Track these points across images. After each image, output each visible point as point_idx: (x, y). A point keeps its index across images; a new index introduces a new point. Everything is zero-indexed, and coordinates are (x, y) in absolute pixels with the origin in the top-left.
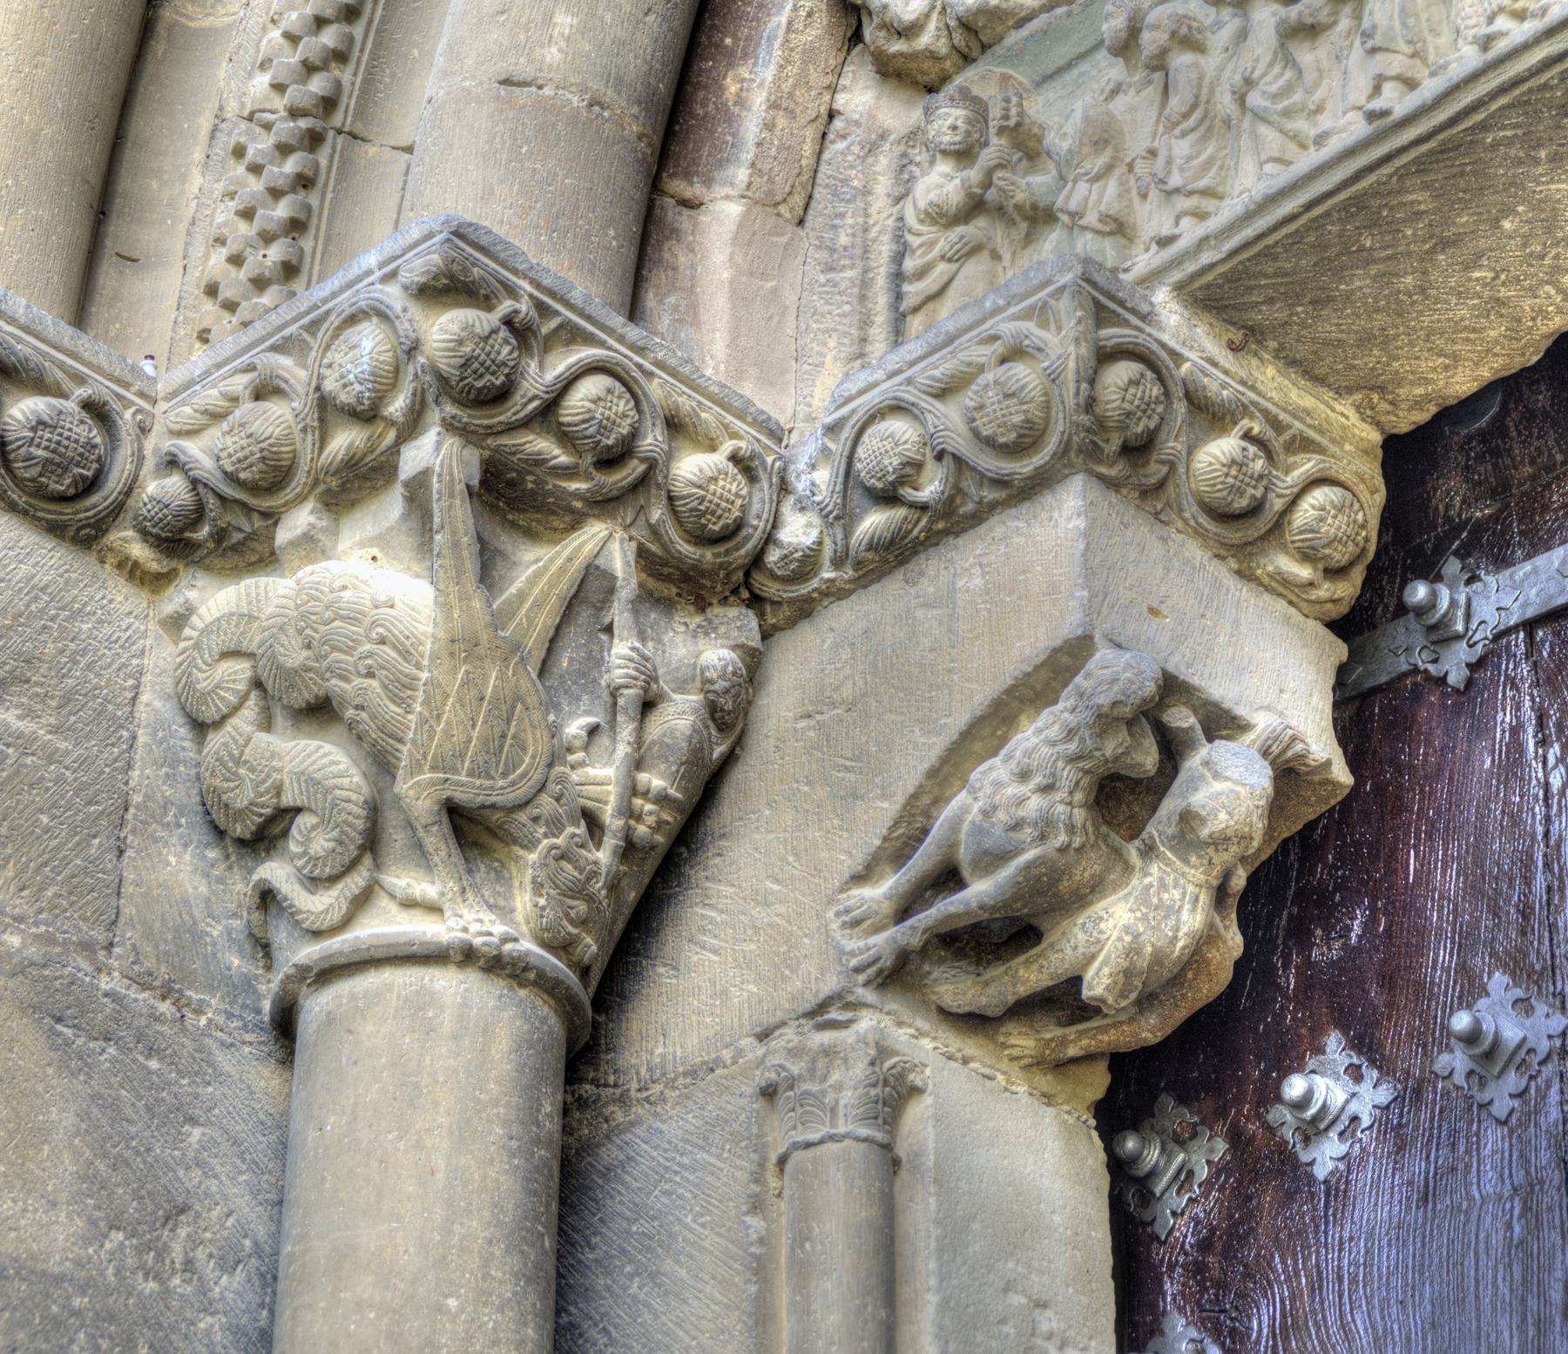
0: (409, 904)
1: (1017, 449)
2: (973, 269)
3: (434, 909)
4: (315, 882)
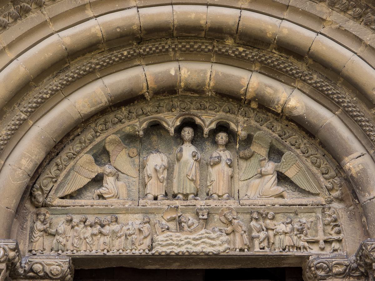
1: (54, 276)
2: (41, 238)
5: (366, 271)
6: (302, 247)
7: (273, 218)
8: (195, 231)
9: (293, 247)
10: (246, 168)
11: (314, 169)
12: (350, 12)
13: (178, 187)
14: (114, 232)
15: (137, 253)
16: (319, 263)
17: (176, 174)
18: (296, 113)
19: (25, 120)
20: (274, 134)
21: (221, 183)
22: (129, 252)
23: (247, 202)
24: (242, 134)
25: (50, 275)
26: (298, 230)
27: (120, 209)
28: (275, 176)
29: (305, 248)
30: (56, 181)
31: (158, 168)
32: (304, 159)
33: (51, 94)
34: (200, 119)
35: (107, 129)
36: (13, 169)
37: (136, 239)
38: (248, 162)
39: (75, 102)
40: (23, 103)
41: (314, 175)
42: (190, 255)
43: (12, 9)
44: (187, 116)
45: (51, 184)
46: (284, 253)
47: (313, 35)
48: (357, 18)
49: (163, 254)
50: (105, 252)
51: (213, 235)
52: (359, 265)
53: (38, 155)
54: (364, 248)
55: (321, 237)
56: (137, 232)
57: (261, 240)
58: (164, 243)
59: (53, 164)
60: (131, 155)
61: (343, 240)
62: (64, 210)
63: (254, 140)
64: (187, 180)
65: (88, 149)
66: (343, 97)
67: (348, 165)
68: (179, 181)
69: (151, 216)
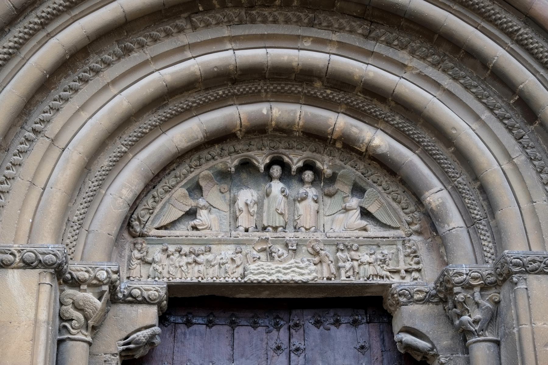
0: (83, 334)
1: (152, 300)
2: (139, 266)
3: (86, 336)
4: (73, 328)
5: (445, 296)
6: (385, 276)
7: (357, 250)
8: (285, 260)
9: (377, 276)
10: (331, 205)
11: (395, 205)
12: (429, 59)
13: (268, 220)
14: (208, 261)
15: (230, 280)
16: (401, 290)
17: (265, 208)
18: (379, 151)
19: (125, 152)
20: (357, 172)
21: (308, 217)
22: (223, 280)
23: (334, 235)
24: (328, 172)
25: (148, 300)
26: (381, 261)
27: (213, 240)
28: (359, 211)
29: (387, 277)
30: (152, 213)
31: (249, 202)
32: (385, 195)
33: (151, 130)
34: (289, 157)
35: (200, 165)
36: (114, 198)
37: (229, 268)
38: (333, 199)
39: (173, 137)
40: (124, 136)
41: (394, 210)
42: (281, 283)
43: (117, 49)
44: (276, 155)
45: (147, 216)
46: (368, 282)
47: (397, 78)
48: (435, 65)
49: (255, 282)
50: (200, 279)
51: (302, 265)
52: (439, 291)
53: (138, 186)
54: (446, 273)
55: (402, 267)
56: (230, 262)
57: (347, 269)
58: (256, 272)
59: (150, 196)
60: (222, 190)
61: (422, 270)
62: (160, 240)
63: (338, 178)
64: (277, 213)
65: (183, 183)
66: (423, 137)
67: (428, 199)
68: (268, 215)
69: (243, 247)
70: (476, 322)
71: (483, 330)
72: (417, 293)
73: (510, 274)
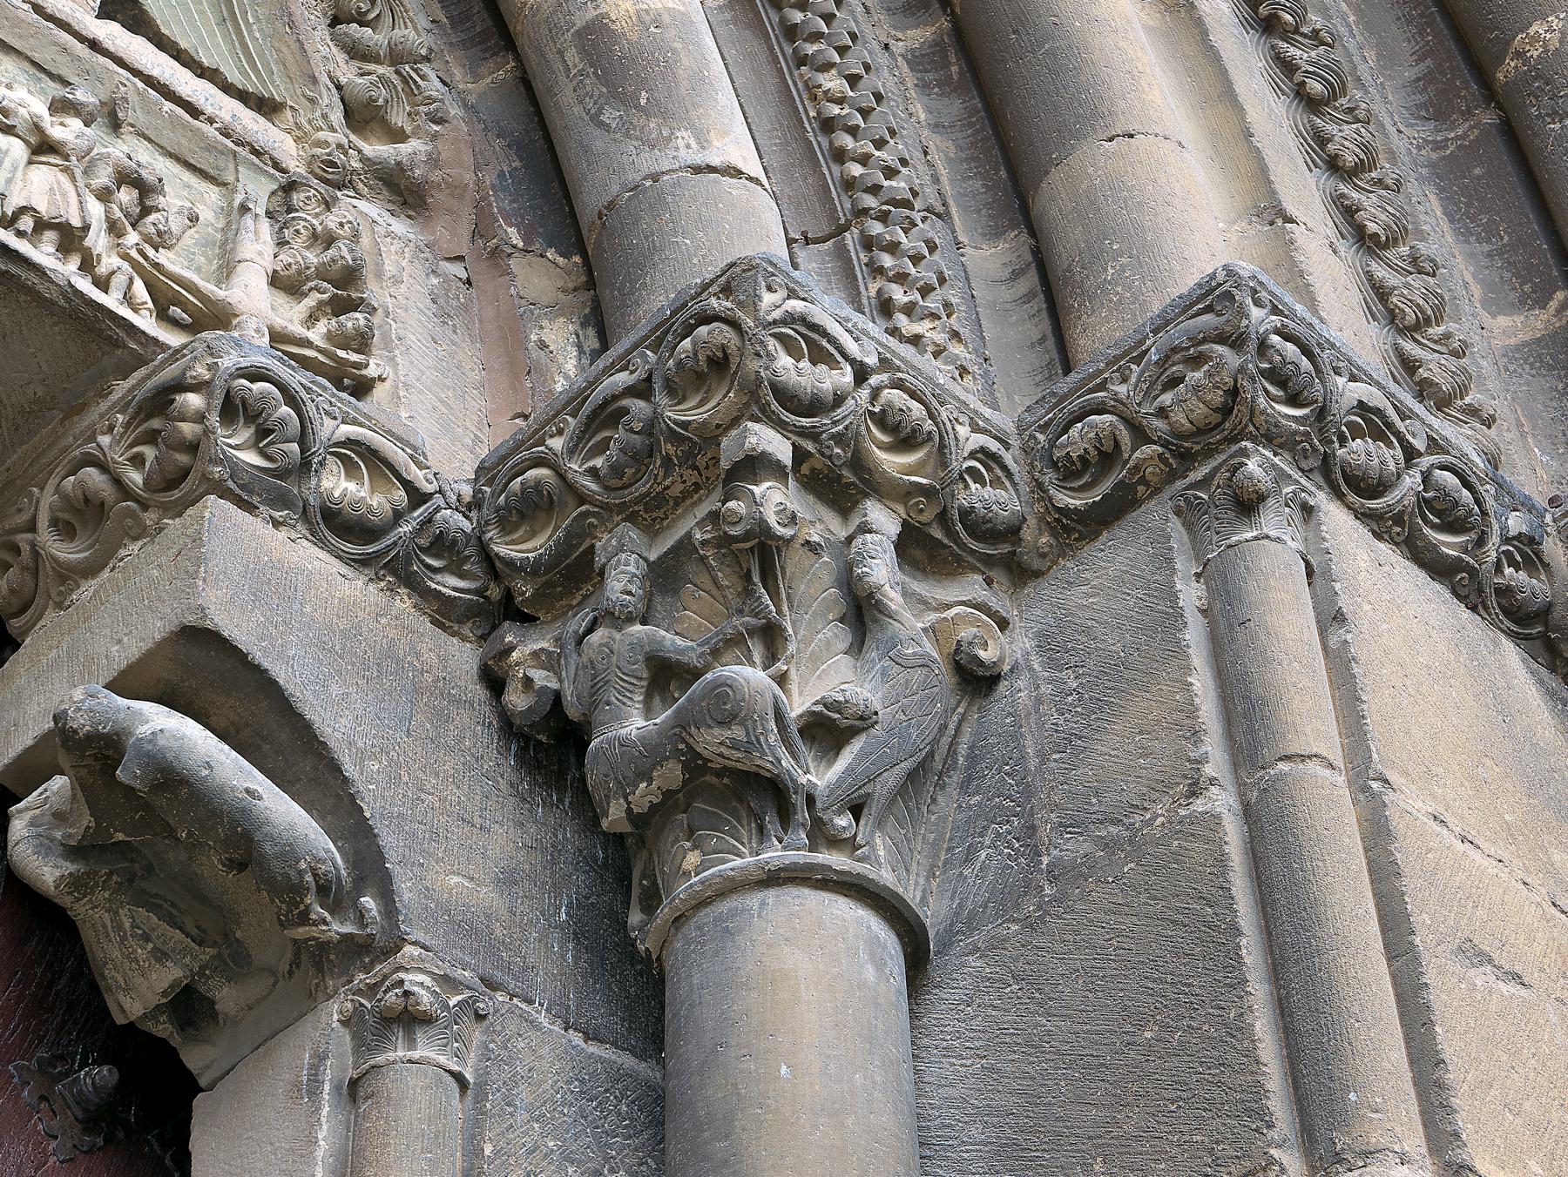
70: (827, 730)
71: (857, 811)
72: (351, 469)
73: (1228, 421)
